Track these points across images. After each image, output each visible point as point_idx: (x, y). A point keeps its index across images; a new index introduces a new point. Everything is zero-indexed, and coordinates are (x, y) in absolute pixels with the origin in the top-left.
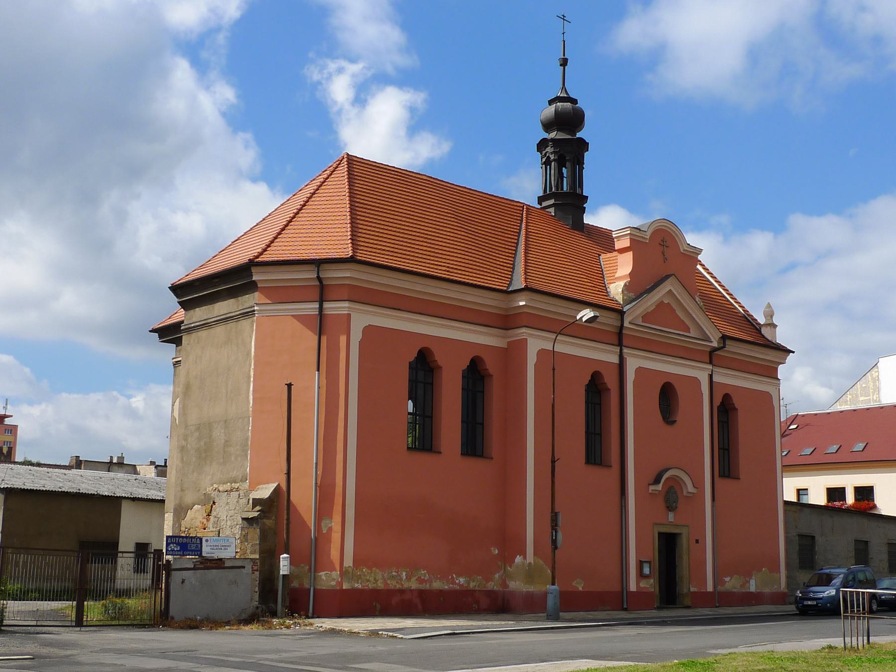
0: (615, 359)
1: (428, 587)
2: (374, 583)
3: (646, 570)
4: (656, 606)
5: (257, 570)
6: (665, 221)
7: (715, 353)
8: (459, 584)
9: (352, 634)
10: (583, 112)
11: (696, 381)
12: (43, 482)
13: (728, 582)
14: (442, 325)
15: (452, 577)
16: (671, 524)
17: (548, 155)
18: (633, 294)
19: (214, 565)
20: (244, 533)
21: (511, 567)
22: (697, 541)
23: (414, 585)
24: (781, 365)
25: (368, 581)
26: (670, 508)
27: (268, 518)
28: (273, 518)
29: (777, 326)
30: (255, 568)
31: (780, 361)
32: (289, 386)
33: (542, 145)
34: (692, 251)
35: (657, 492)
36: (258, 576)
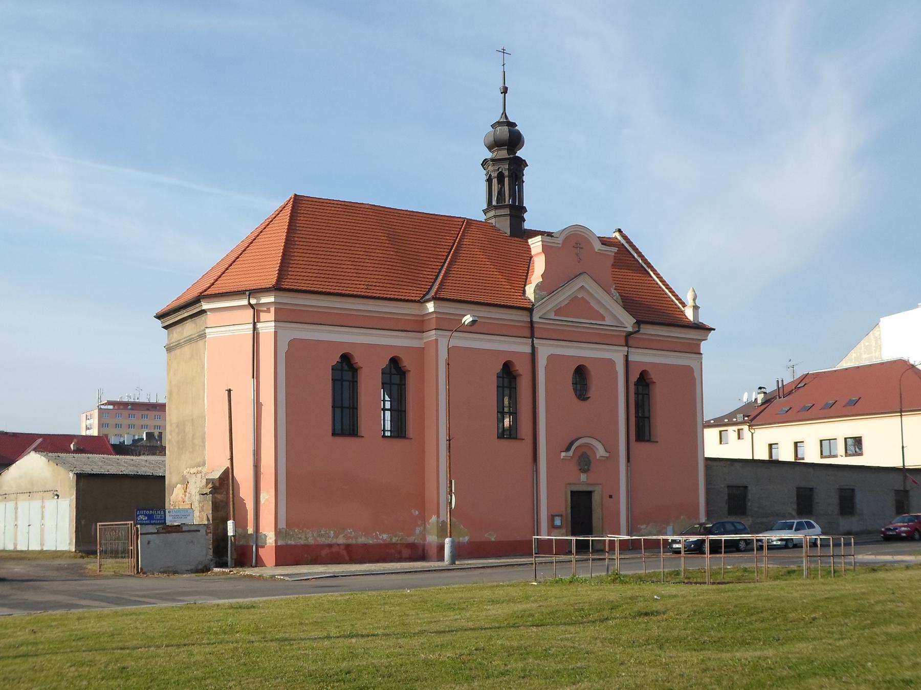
0: (528, 350)
1: (354, 542)
2: (305, 540)
3: (558, 522)
4: (567, 551)
5: (211, 533)
6: (577, 227)
7: (632, 336)
8: (382, 539)
9: (251, 577)
10: (520, 133)
11: (611, 363)
12: (109, 467)
13: (644, 529)
14: (362, 333)
15: (376, 534)
16: (583, 483)
17: (500, 170)
18: (546, 293)
19: (174, 530)
20: (201, 505)
21: (429, 525)
22: (611, 497)
23: (341, 540)
24: (703, 342)
25: (300, 538)
26: (583, 471)
27: (221, 493)
28: (225, 493)
29: (699, 307)
30: (208, 531)
31: (699, 338)
32: (229, 391)
33: (485, 163)
34: (606, 249)
35: (569, 458)
36: (212, 537)
